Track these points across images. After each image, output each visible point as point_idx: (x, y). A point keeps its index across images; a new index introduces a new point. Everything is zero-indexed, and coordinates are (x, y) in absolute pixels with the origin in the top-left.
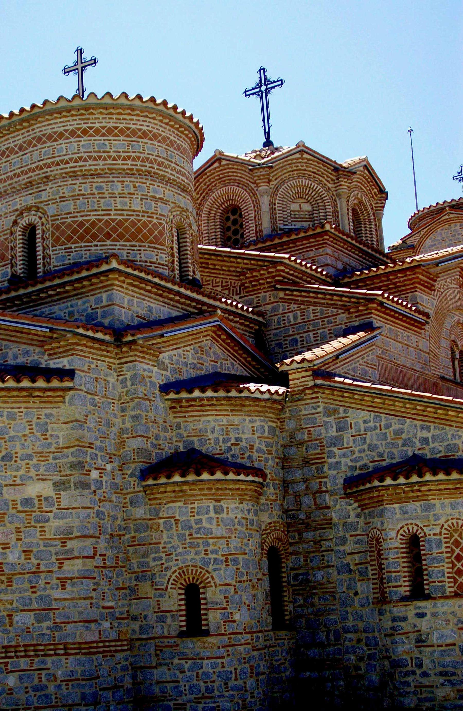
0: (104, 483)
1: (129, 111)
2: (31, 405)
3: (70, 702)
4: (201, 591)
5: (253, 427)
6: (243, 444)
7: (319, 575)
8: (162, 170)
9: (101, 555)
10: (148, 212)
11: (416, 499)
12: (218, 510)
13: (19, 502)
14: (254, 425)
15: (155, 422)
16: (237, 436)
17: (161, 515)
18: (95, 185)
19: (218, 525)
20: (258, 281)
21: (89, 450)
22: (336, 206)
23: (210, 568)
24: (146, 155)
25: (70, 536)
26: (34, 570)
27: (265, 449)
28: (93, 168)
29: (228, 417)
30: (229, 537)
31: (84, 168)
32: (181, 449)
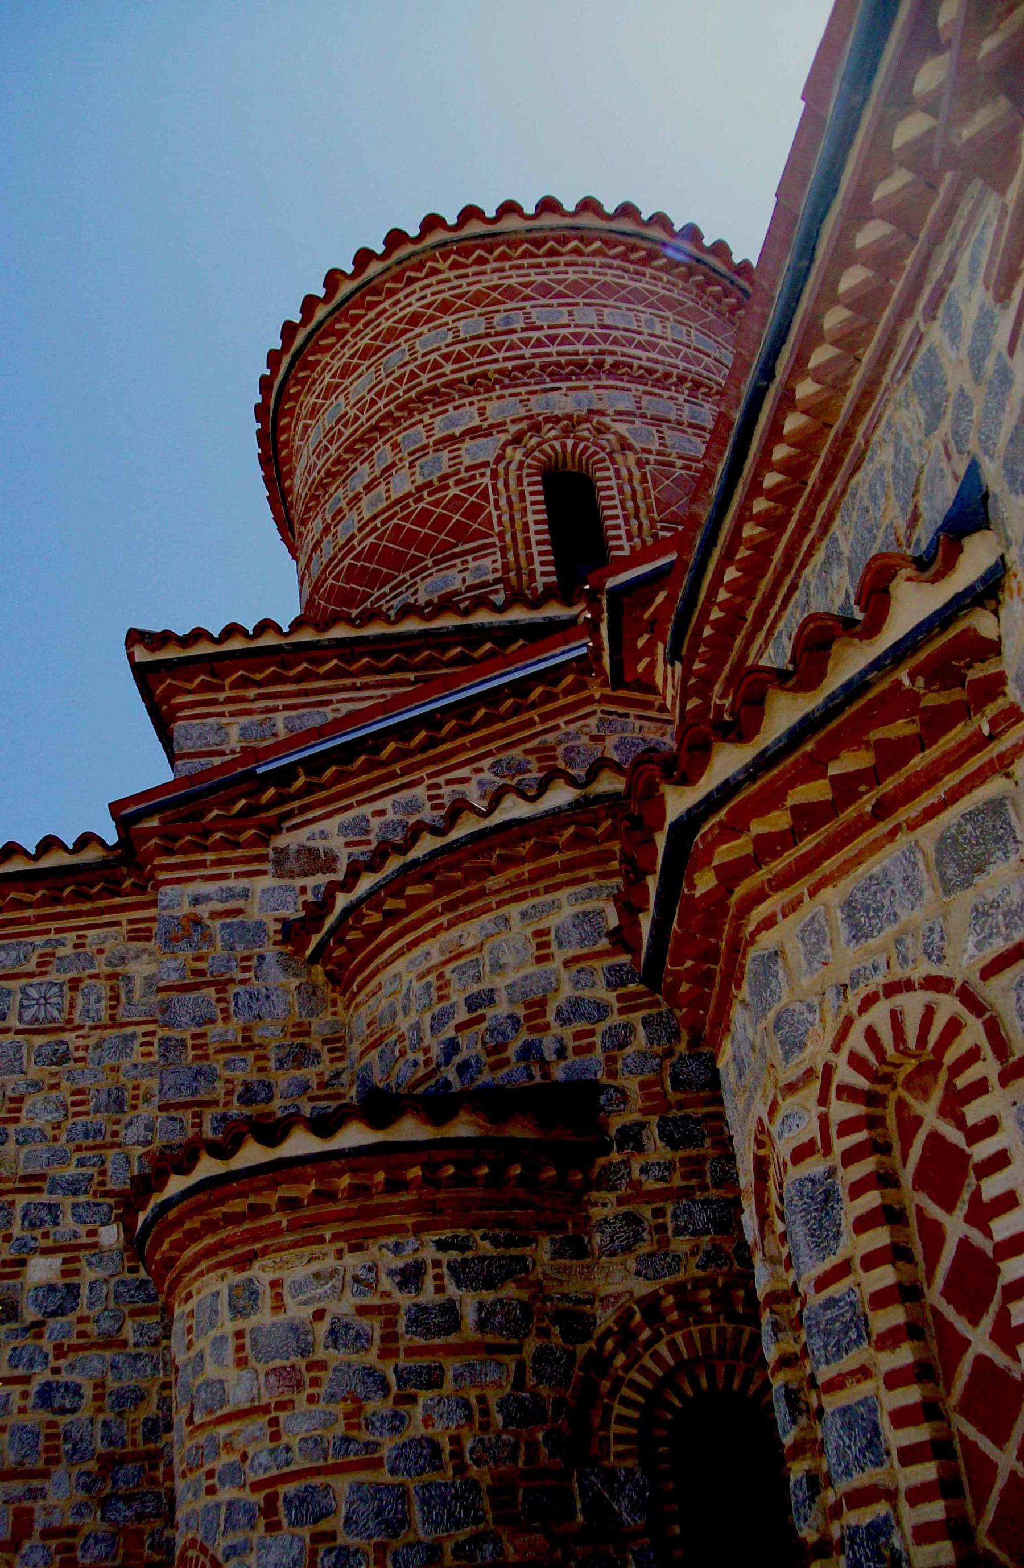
0: (85, 1291)
5: (538, 933)
6: (502, 1009)
8: (472, 366)
9: (48, 1533)
10: (430, 484)
14: (551, 921)
15: (248, 1043)
16: (474, 988)
19: (241, 1362)
21: (22, 1200)
24: (420, 361)
27: (611, 996)
29: (443, 936)
30: (281, 1406)
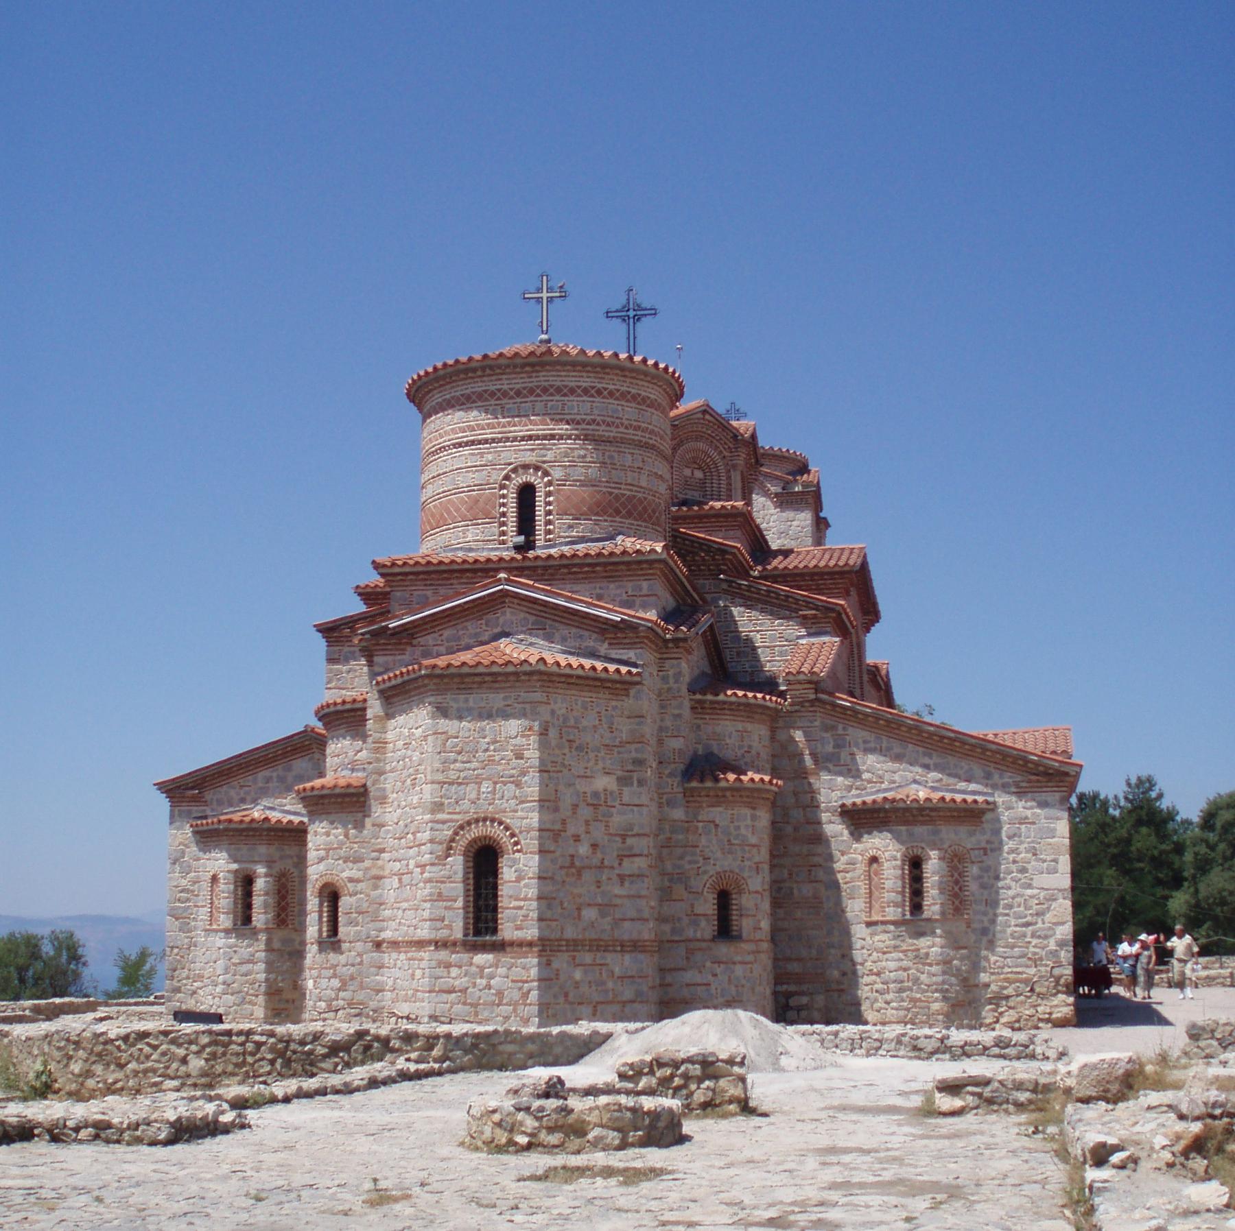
1: (642, 377)
2: (600, 695)
3: (624, 999)
4: (734, 896)
7: (807, 890)
11: (923, 823)
12: (754, 818)
13: (589, 795)
17: (700, 818)
18: (607, 453)
20: (699, 566)
22: (729, 478)
23: (746, 874)
25: (630, 833)
26: (599, 864)
28: (607, 434)
31: (597, 433)
32: (700, 752)
